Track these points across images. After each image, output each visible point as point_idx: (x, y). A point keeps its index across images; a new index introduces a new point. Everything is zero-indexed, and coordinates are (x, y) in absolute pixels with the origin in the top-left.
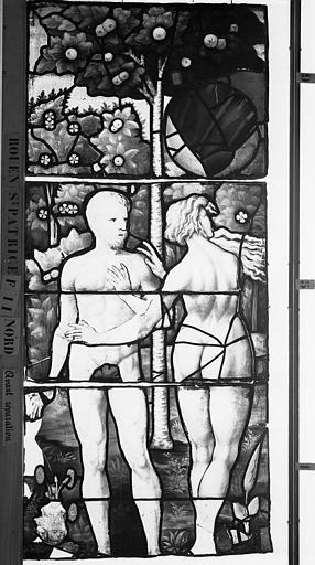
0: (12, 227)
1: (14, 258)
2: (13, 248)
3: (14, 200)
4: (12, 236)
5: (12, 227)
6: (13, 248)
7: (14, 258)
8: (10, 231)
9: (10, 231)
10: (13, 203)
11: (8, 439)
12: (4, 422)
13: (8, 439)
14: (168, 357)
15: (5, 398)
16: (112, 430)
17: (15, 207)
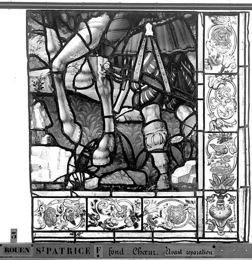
0: (59, 251)
1: (80, 249)
2: (73, 251)
3: (41, 250)
4: (65, 251)
5: (59, 251)
6: (73, 251)
7: (80, 249)
8: (62, 253)
9: (62, 253)
10: (43, 251)
11: (211, 253)
12: (202, 255)
13: (211, 253)
14: (247, 147)
15: (184, 254)
16: (159, 150)
17: (46, 250)
